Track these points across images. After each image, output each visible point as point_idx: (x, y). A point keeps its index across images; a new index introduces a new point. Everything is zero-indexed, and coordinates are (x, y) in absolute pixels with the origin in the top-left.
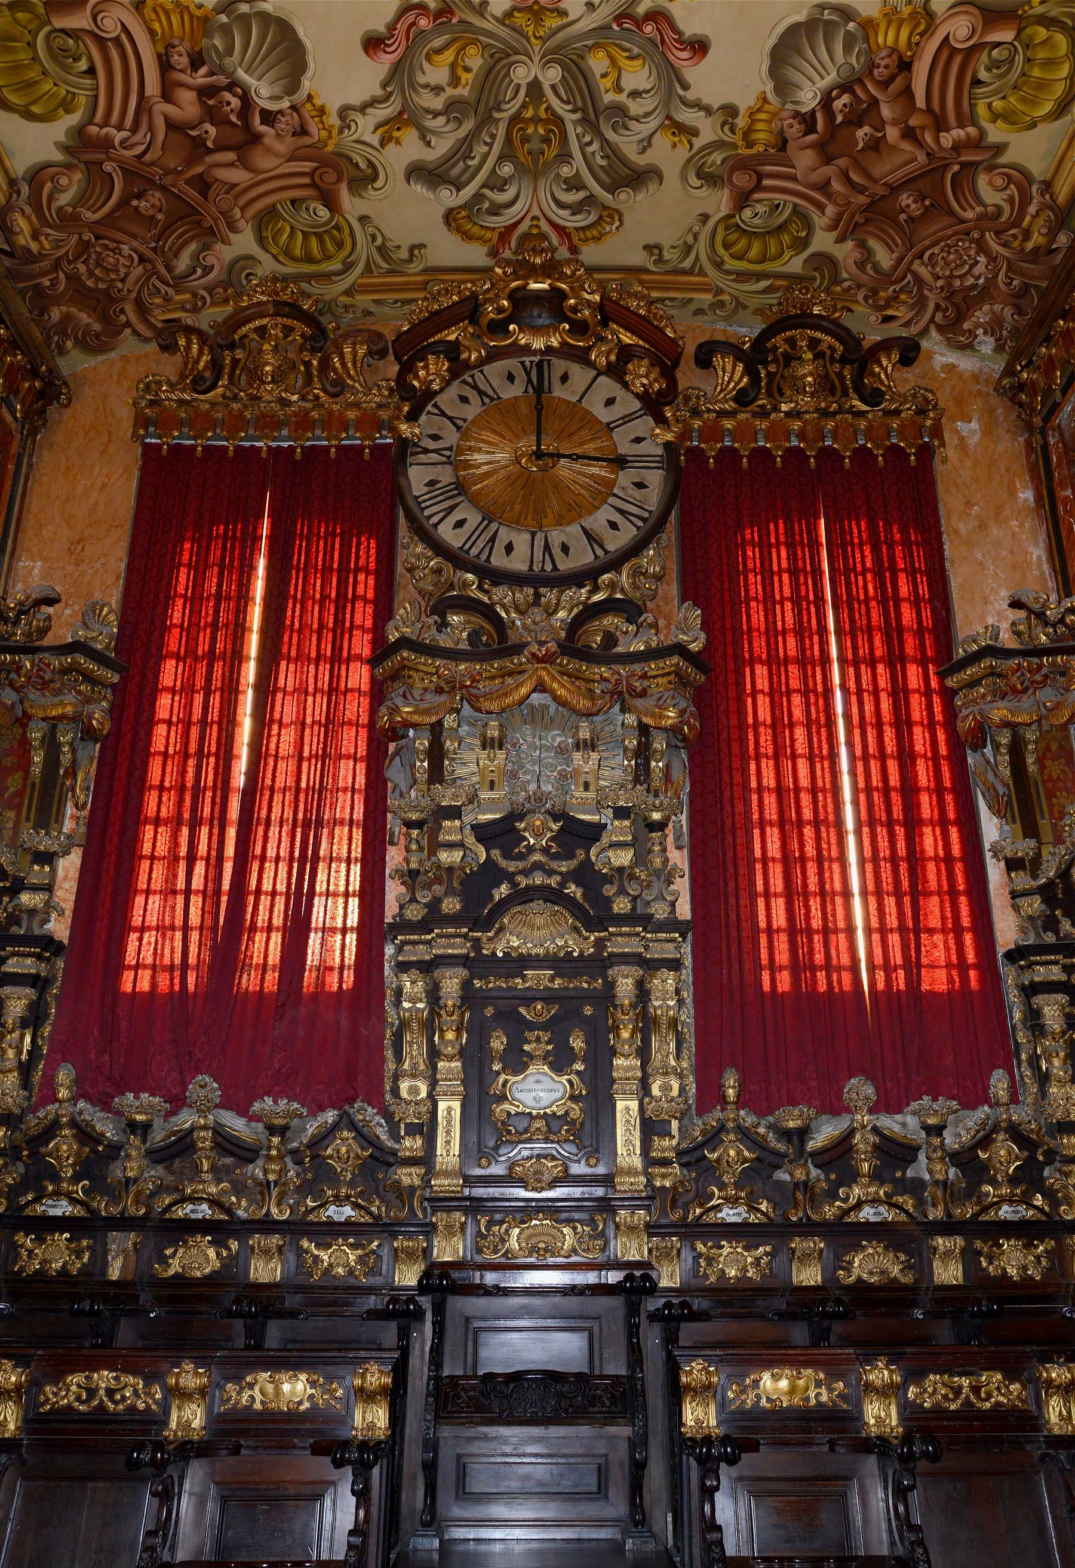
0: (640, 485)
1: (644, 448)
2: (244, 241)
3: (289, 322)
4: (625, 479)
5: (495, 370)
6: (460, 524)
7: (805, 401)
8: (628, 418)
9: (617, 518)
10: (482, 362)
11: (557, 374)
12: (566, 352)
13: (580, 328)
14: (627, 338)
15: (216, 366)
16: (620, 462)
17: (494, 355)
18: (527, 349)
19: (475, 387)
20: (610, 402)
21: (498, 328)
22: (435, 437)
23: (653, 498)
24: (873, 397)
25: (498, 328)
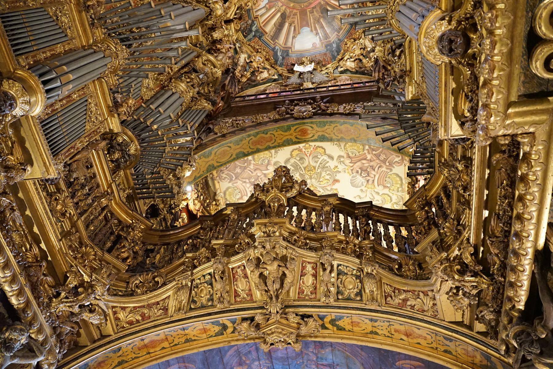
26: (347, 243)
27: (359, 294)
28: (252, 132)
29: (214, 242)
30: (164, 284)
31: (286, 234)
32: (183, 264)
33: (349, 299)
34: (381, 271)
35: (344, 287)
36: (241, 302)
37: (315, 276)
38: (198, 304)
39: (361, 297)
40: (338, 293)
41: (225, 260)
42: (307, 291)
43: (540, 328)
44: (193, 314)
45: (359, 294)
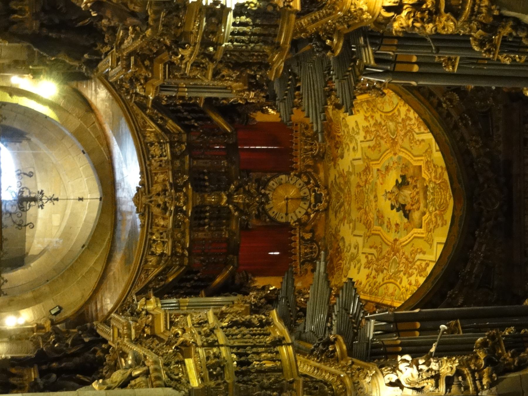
0: (282, 217)
1: (290, 219)
2: (328, 144)
3: (317, 150)
4: (284, 215)
5: (306, 190)
6: (273, 184)
7: (303, 251)
8: (296, 215)
9: (275, 213)
10: (308, 188)
11: (306, 202)
12: (310, 204)
13: (315, 206)
14: (312, 216)
15: (308, 137)
16: (287, 214)
17: (309, 190)
18: (310, 196)
19: (303, 186)
20: (300, 212)
21: (314, 191)
22: (291, 180)
23: (280, 220)
24: (303, 263)
25: (314, 191)
26: (183, 248)
27: (153, 254)
28: (447, 139)
29: (188, 156)
30: (159, 126)
31: (184, 208)
32: (180, 133)
33: (150, 247)
34: (161, 268)
35: (157, 244)
36: (151, 177)
37: (163, 226)
38: (151, 148)
39: (151, 255)
40: (154, 241)
41: (170, 167)
42: (157, 221)
43: (85, 335)
44: (143, 146)
45: (153, 254)
